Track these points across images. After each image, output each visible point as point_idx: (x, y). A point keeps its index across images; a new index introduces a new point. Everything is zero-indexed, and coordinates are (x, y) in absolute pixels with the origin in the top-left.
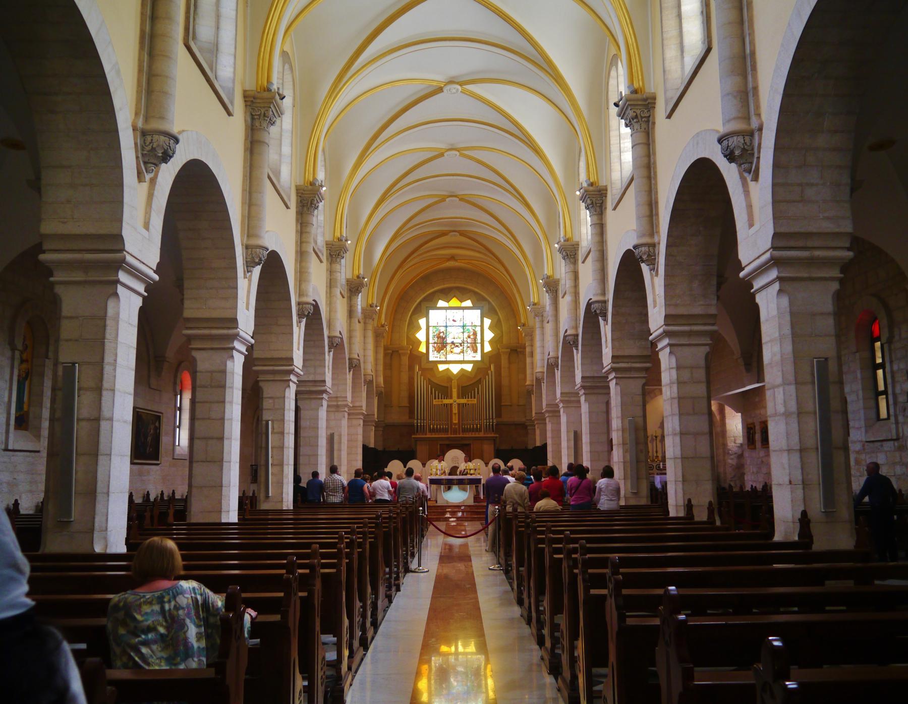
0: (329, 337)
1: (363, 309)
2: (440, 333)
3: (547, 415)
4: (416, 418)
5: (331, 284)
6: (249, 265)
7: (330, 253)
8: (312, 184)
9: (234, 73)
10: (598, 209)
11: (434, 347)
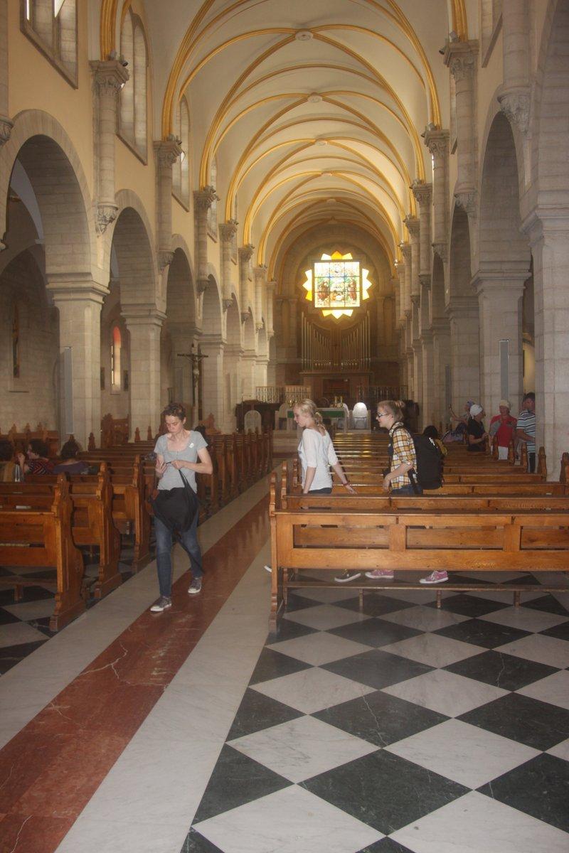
0: (223, 300)
1: (255, 270)
2: (324, 283)
3: (408, 356)
5: (224, 258)
6: (162, 265)
8: (205, 189)
9: (147, 135)
10: (426, 202)
11: (319, 295)
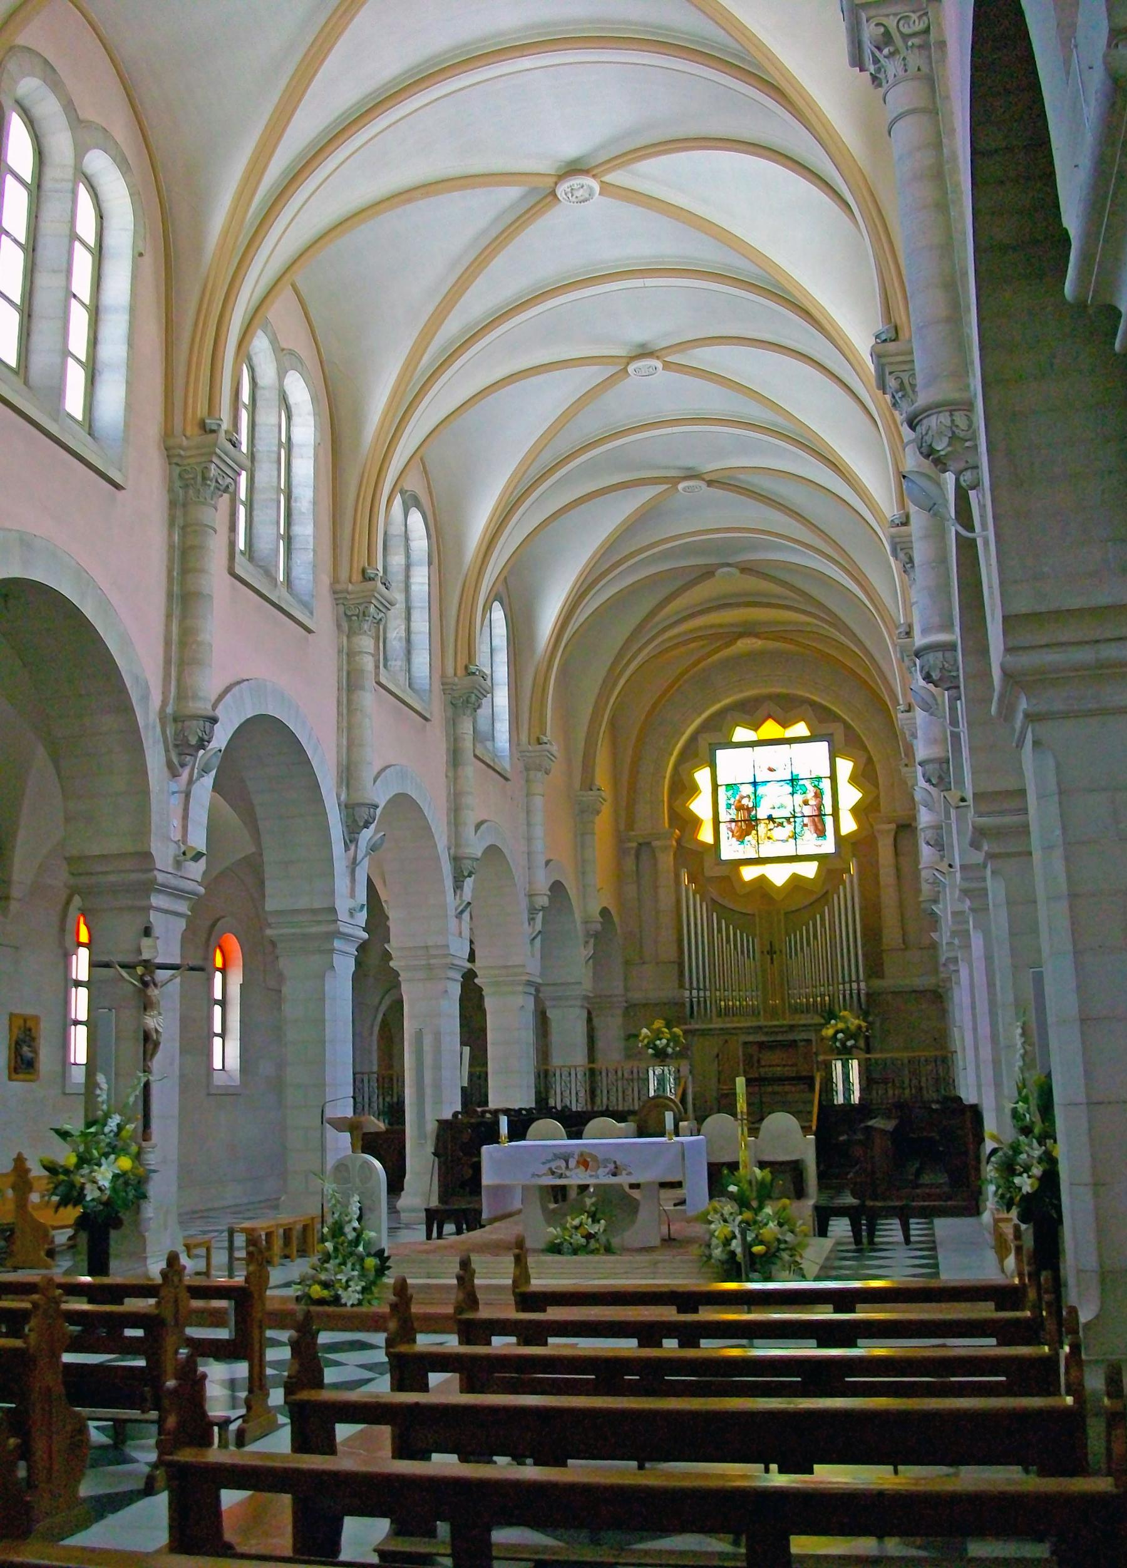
2: (743, 797)
4: (687, 985)
7: (345, 614)
